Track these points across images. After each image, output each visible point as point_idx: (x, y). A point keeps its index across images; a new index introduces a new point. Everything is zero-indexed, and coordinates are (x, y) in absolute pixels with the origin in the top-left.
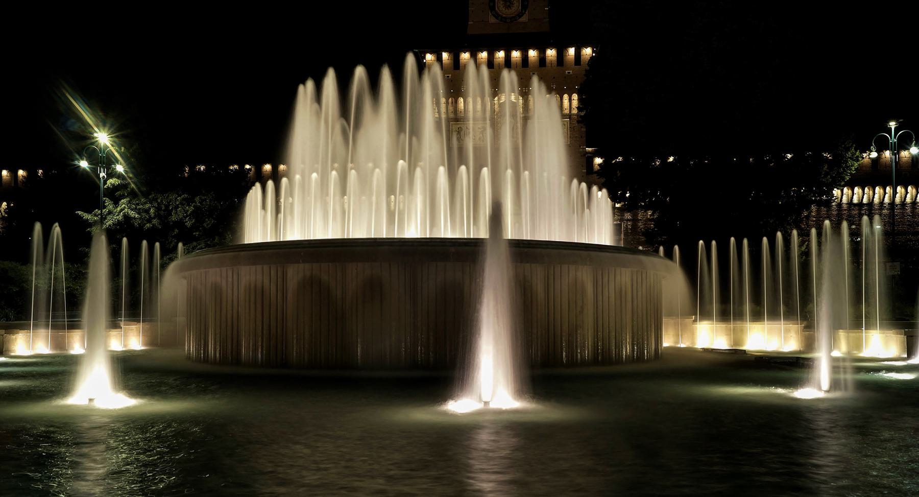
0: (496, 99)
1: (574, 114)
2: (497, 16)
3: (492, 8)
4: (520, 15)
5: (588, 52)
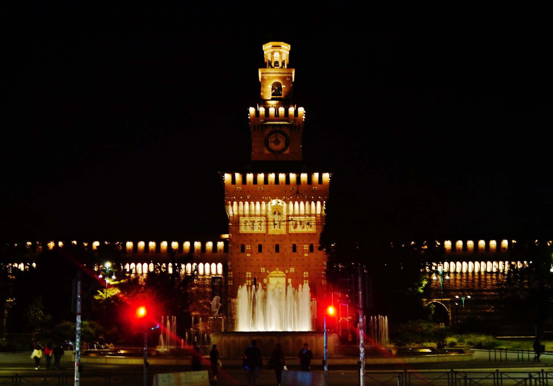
0: (269, 203)
1: (318, 214)
2: (269, 149)
3: (267, 145)
4: (284, 150)
5: (326, 176)
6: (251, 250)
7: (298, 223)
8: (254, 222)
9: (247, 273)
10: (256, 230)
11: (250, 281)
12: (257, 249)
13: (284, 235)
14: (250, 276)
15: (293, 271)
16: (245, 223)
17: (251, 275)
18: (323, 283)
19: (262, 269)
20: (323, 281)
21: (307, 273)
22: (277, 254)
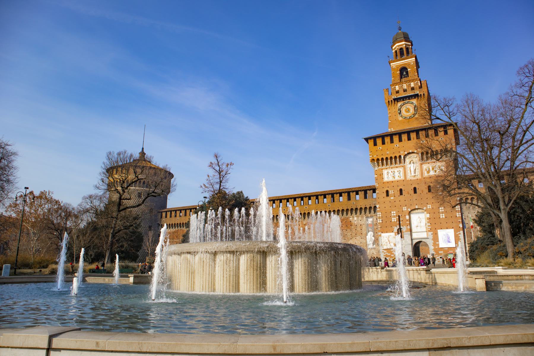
6: (394, 193)
7: (431, 169)
8: (394, 171)
9: (392, 212)
10: (397, 178)
11: (395, 218)
12: (399, 192)
13: (420, 179)
14: (395, 215)
15: (430, 207)
16: (388, 174)
17: (396, 213)
18: (458, 216)
19: (404, 208)
20: (457, 214)
21: (443, 208)
22: (415, 194)
